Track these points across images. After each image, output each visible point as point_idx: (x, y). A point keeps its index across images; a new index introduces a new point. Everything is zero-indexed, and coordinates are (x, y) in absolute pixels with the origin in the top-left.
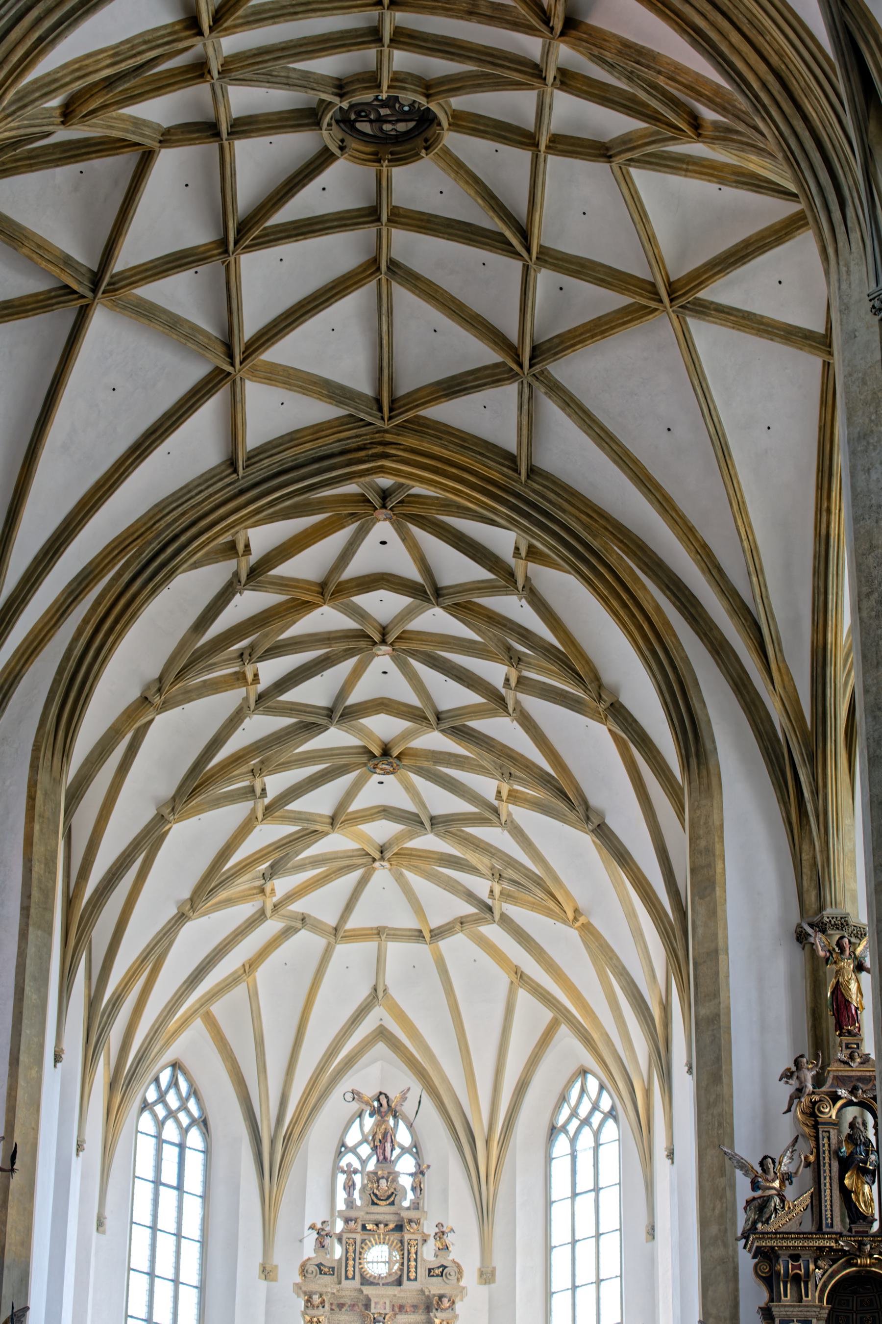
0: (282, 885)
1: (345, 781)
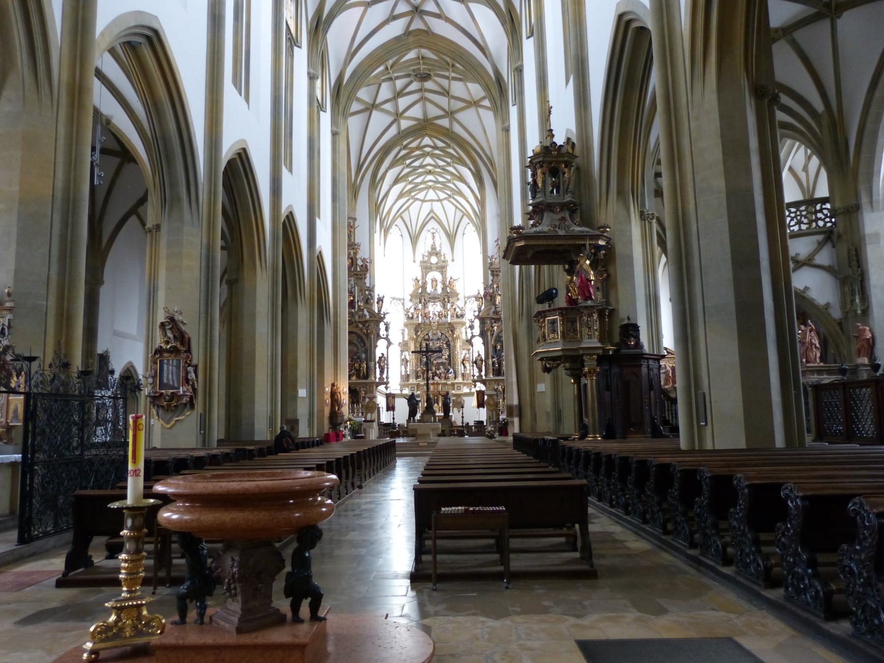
0: (413, 194)
1: (423, 177)
